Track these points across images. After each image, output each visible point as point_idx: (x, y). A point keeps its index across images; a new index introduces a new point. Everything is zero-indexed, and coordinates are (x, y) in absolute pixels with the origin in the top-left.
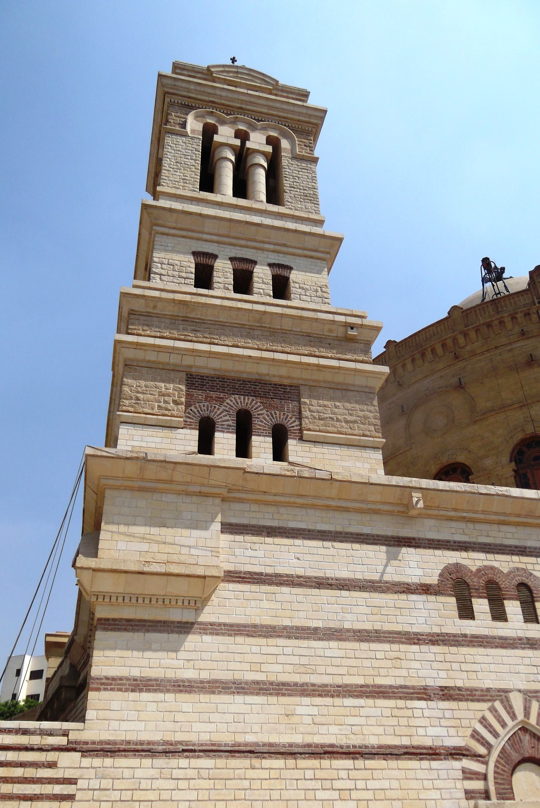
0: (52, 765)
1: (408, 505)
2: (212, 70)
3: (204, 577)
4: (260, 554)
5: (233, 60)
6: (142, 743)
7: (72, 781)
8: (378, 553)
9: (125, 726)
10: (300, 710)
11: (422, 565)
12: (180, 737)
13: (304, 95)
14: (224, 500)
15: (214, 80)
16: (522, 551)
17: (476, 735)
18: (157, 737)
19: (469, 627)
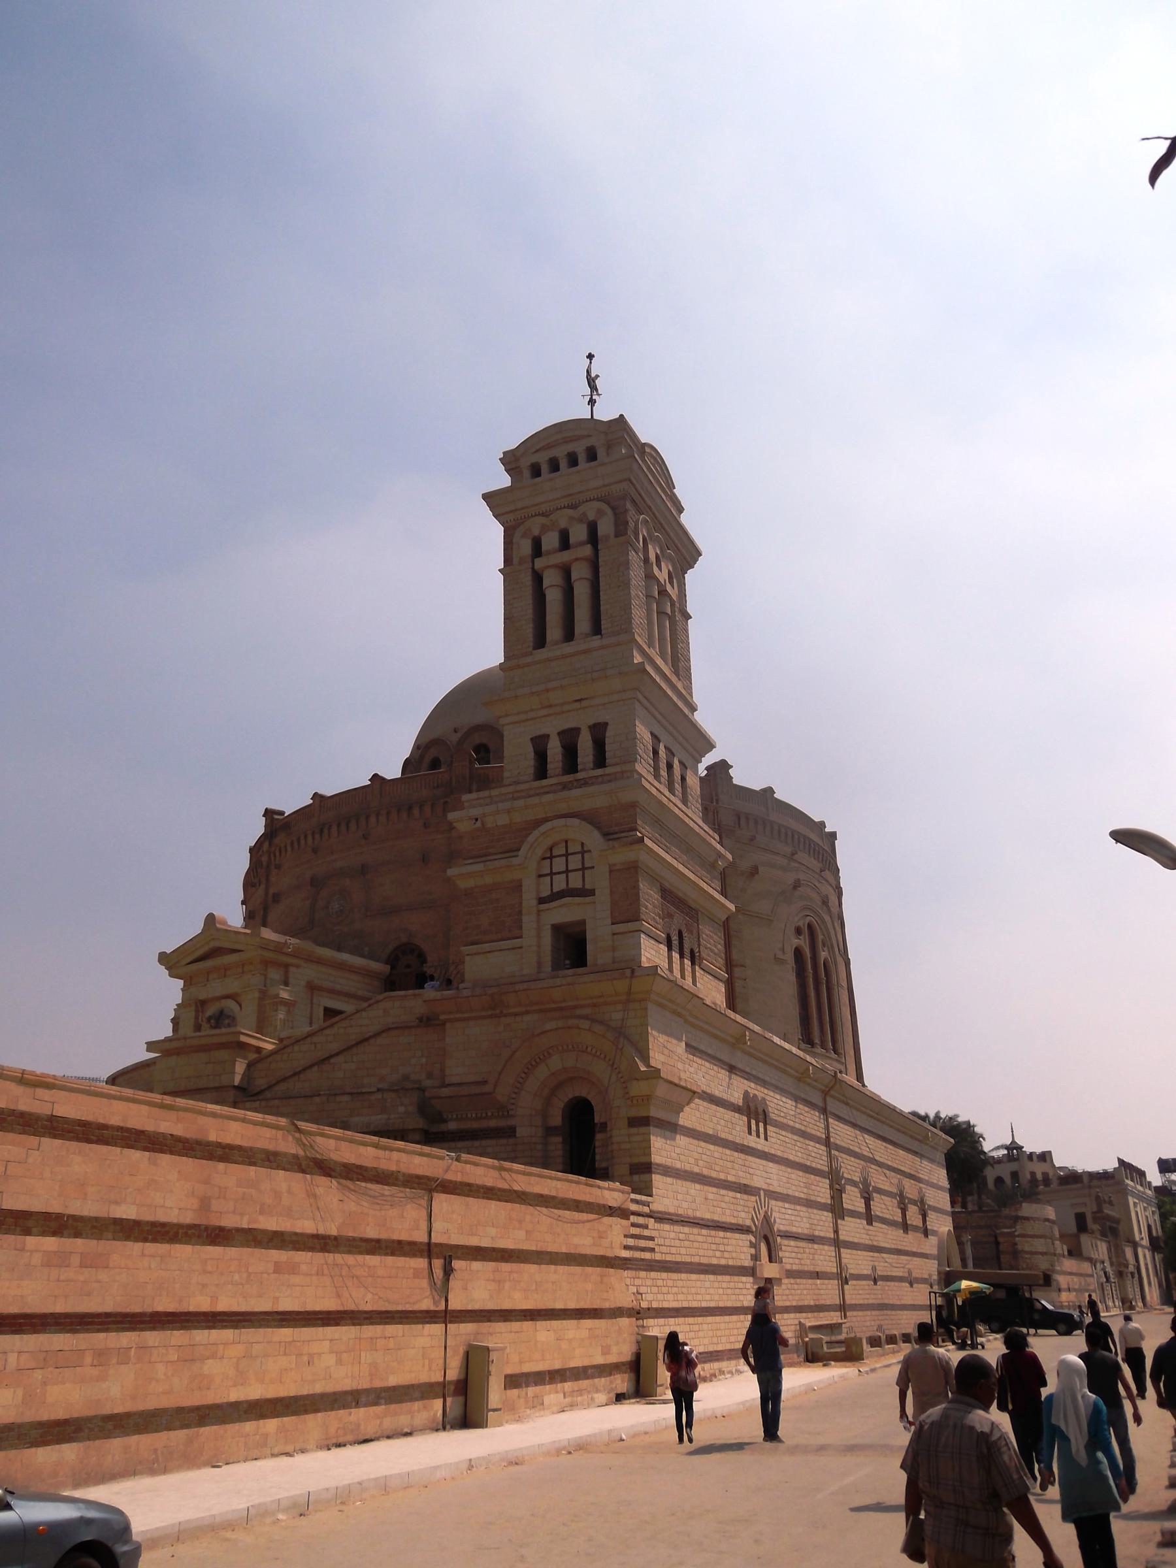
0: (646, 1227)
1: (741, 1039)
2: (647, 450)
3: (694, 1092)
4: (692, 1070)
5: (590, 356)
6: (669, 1214)
7: (652, 1239)
8: (723, 1074)
9: (666, 1201)
10: (710, 1196)
11: (736, 1089)
12: (680, 1212)
13: (681, 510)
14: (686, 1021)
15: (644, 461)
16: (764, 1083)
17: (753, 1219)
18: (672, 1210)
19: (752, 1141)
